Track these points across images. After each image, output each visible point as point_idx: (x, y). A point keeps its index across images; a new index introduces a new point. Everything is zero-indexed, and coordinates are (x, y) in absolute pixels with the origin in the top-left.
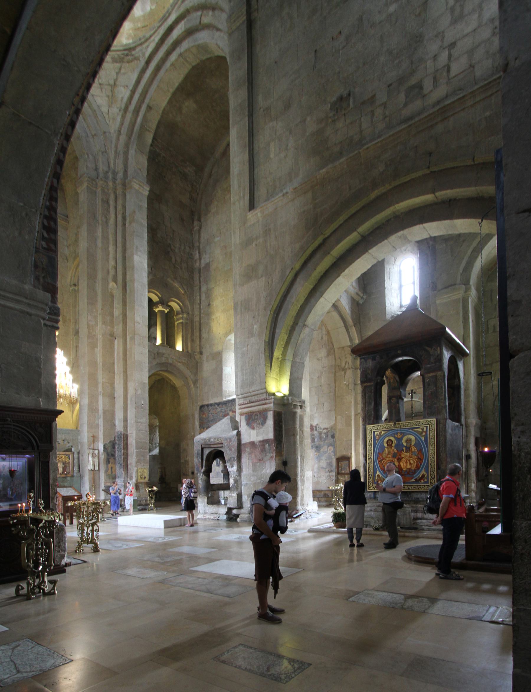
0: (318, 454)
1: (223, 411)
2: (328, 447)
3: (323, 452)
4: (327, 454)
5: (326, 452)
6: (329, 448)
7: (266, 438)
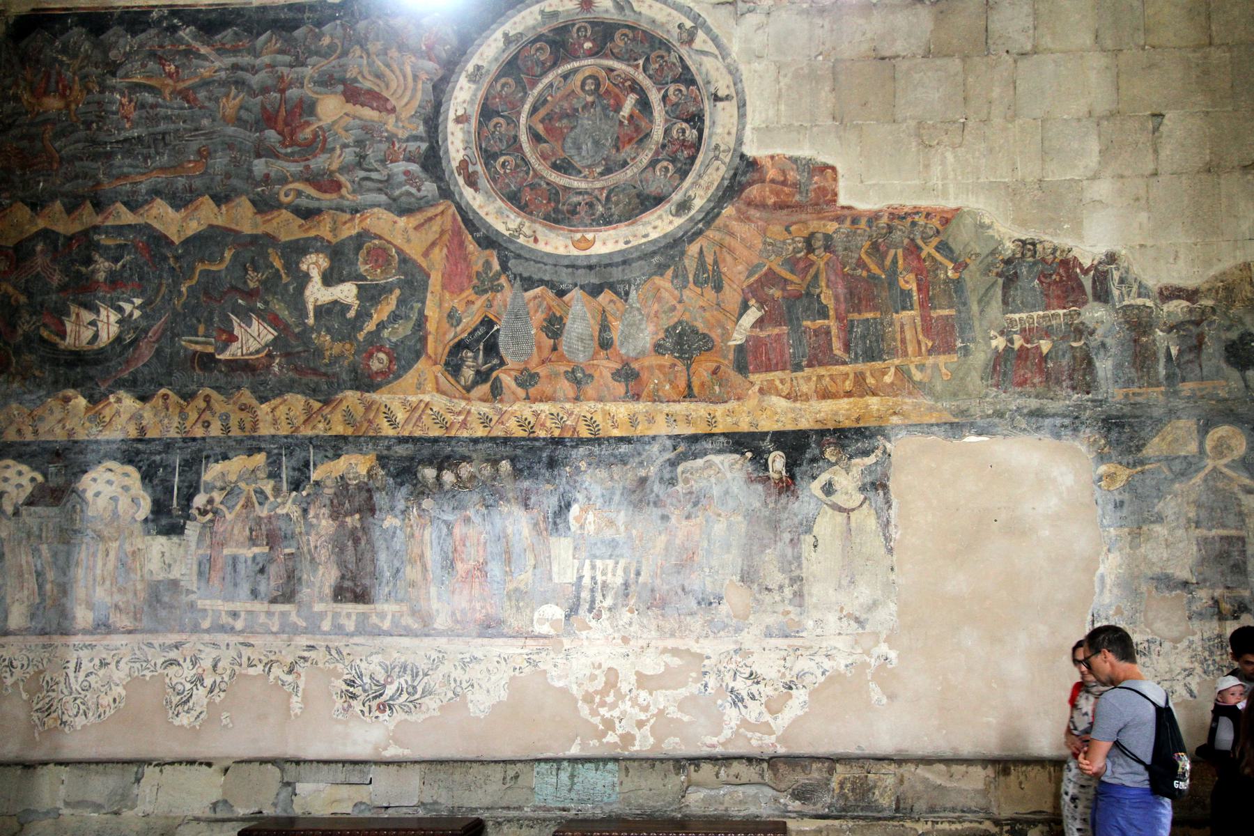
0: (1123, 474)
1: (254, 80)
2: (1204, 430)
3: (1169, 460)
4: (1198, 479)
5: (1188, 467)
6: (1223, 431)
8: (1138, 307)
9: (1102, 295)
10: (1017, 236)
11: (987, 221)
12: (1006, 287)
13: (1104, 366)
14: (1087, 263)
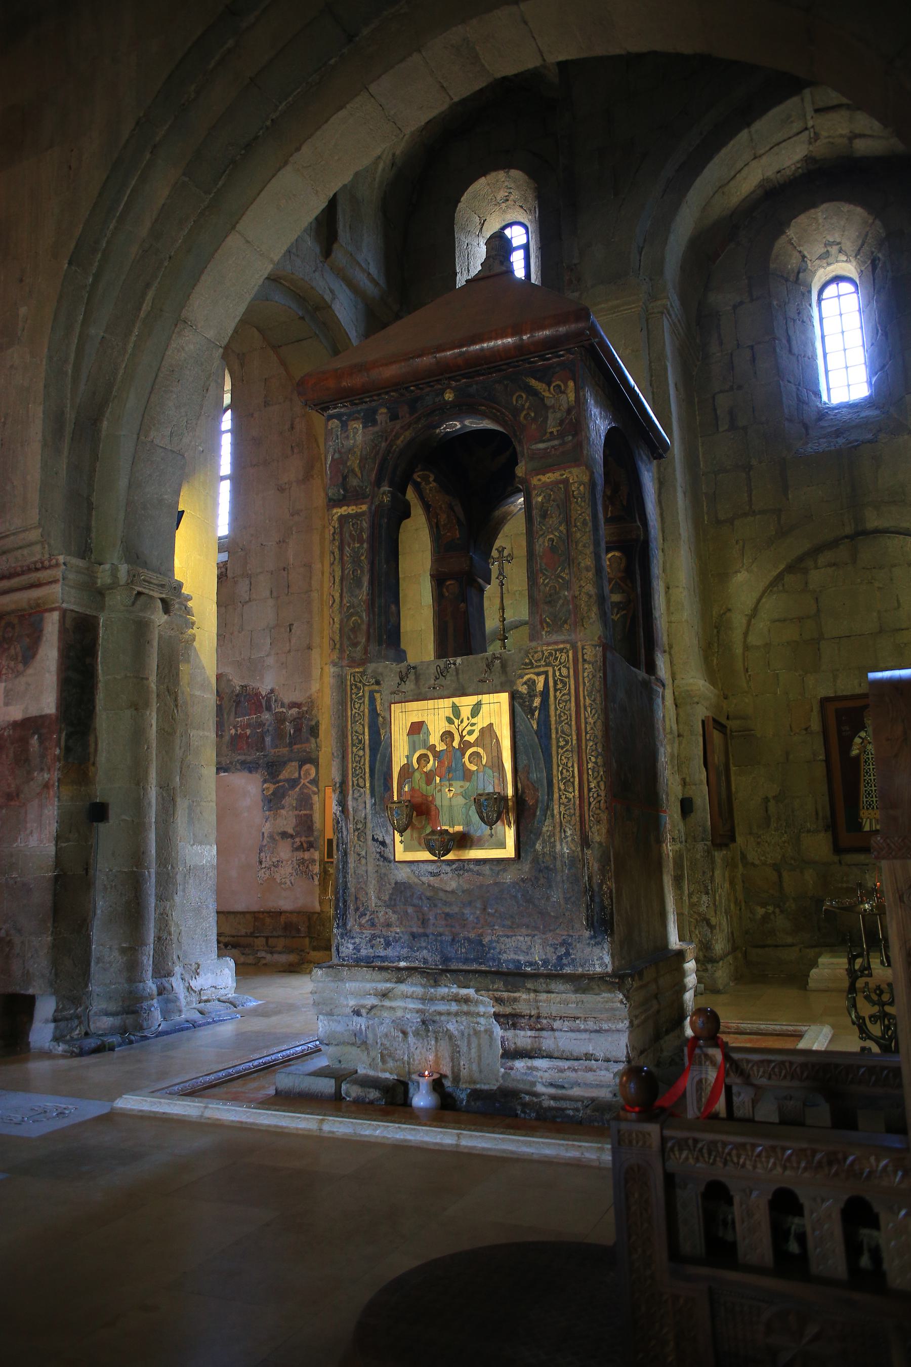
7: (33, 712)
8: (280, 713)
9: (269, 708)
10: (240, 684)
11: (231, 678)
12: (236, 707)
13: (268, 740)
14: (264, 694)
